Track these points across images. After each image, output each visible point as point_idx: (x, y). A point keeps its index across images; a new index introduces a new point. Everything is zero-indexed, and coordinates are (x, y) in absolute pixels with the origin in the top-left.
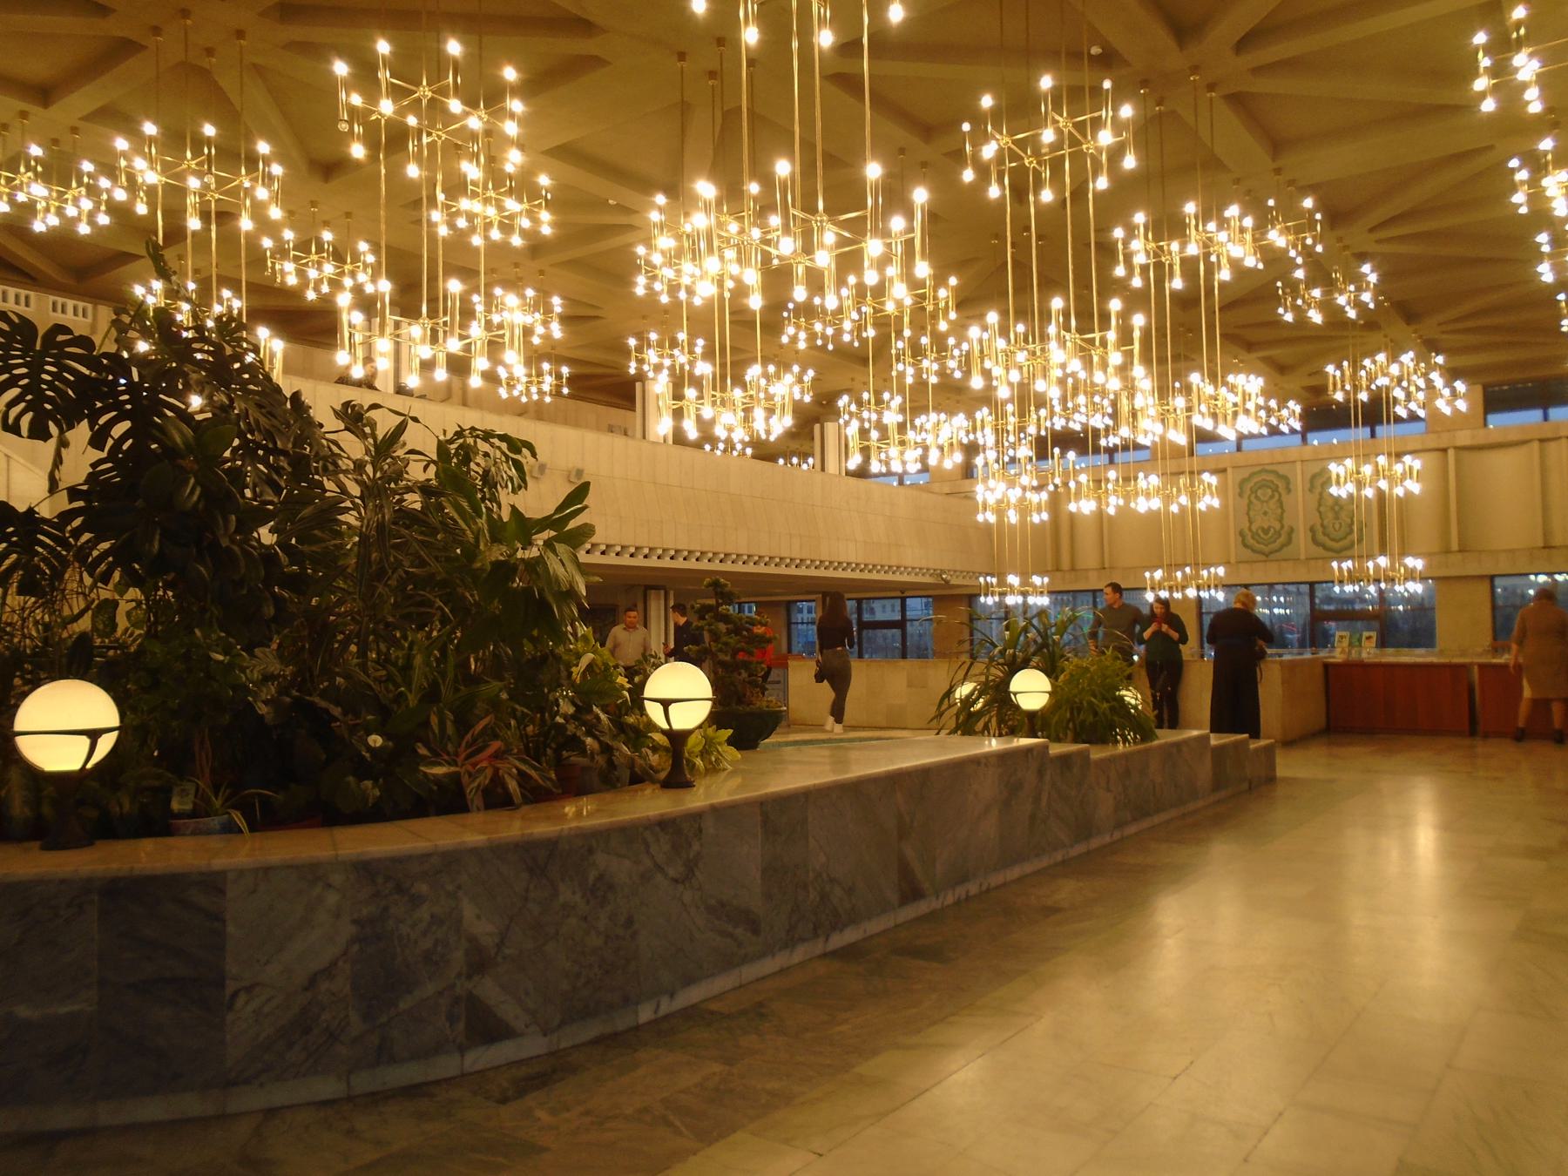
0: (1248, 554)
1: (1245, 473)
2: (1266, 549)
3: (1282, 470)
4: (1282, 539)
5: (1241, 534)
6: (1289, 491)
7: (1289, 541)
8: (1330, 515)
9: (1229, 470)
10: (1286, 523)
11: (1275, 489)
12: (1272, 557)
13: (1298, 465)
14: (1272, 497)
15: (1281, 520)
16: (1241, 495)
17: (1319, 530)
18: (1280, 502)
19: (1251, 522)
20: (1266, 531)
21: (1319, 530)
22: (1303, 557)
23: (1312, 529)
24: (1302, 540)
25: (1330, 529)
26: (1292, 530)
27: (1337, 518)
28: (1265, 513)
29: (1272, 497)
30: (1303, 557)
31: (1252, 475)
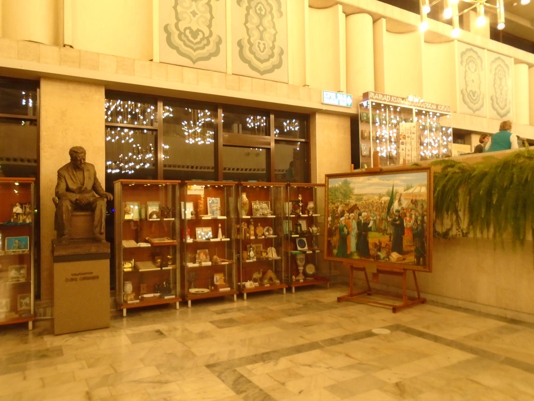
0: (174, 57)
2: (195, 54)
4: (211, 48)
5: (166, 28)
8: (256, 34)
12: (200, 64)
15: (210, 26)
17: (247, 46)
19: (178, 19)
20: (195, 34)
21: (247, 46)
22: (230, 71)
23: (240, 44)
24: (229, 49)
25: (255, 48)
27: (261, 38)
28: (194, 14)
30: (230, 71)
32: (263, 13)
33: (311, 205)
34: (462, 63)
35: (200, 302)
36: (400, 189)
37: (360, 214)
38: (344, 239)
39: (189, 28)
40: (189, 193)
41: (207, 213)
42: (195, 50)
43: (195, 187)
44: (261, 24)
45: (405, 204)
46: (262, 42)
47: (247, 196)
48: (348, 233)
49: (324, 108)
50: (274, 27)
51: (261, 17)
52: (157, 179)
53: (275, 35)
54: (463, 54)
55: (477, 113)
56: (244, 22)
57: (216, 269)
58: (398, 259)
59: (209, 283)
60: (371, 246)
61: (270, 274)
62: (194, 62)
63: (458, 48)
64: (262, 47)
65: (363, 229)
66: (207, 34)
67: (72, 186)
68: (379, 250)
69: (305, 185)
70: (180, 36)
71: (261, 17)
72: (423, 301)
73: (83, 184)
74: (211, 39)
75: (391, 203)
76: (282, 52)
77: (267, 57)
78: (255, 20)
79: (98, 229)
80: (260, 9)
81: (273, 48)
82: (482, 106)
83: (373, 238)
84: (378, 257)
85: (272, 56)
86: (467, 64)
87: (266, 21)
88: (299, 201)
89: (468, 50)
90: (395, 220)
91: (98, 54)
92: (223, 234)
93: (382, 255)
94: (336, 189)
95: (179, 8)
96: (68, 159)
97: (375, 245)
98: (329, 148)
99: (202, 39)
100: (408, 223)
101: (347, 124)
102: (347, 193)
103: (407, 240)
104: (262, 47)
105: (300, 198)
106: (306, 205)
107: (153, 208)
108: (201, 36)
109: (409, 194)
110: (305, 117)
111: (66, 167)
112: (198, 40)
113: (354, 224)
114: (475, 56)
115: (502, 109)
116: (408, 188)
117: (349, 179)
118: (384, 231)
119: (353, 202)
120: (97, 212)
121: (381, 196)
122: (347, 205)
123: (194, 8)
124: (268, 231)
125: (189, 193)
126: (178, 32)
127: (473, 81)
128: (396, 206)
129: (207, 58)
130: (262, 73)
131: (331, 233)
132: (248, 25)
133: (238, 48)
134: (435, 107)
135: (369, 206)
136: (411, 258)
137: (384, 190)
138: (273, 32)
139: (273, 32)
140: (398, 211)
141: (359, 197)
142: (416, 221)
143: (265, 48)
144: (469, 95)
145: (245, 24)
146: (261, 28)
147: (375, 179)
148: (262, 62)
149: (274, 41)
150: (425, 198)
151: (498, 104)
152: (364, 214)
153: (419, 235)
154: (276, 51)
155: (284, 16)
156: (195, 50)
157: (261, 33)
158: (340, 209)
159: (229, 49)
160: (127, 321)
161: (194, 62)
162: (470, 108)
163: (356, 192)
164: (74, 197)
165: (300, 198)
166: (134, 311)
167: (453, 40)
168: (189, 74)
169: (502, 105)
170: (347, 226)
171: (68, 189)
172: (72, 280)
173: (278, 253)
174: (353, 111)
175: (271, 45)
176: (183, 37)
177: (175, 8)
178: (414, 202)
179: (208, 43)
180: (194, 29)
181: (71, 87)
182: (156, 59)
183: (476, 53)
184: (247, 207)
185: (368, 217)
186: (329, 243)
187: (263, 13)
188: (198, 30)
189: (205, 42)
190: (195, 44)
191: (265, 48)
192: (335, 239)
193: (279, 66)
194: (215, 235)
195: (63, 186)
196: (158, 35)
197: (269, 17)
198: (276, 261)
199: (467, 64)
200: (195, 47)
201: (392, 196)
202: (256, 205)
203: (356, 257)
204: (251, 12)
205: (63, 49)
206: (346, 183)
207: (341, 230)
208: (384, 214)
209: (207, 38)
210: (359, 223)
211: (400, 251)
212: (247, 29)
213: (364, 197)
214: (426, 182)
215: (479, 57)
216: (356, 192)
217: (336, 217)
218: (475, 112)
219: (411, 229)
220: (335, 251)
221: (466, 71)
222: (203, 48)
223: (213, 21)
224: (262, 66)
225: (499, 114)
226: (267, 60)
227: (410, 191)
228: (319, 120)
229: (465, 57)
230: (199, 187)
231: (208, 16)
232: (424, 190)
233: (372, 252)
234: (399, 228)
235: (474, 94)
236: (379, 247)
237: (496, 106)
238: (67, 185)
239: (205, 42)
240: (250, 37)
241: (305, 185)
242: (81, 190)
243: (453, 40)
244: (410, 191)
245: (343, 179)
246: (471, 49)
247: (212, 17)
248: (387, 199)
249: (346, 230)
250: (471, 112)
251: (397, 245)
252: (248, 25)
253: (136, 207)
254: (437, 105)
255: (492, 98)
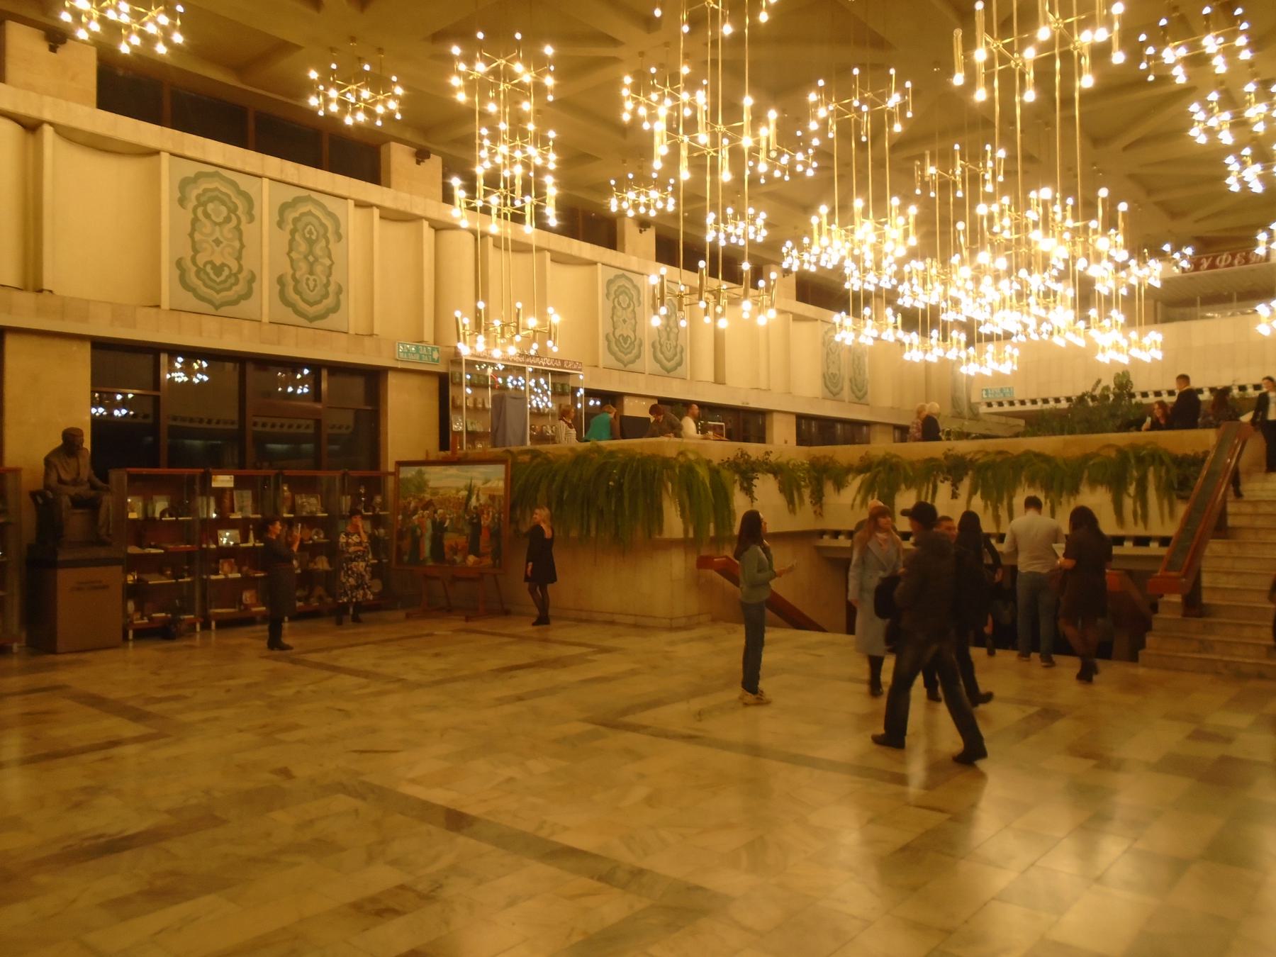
0: (191, 302)
1: (191, 169)
2: (218, 298)
3: (244, 183)
4: (240, 288)
5: (179, 264)
6: (251, 219)
7: (247, 295)
8: (303, 266)
9: (165, 157)
10: (248, 264)
11: (233, 210)
12: (225, 310)
13: (266, 181)
14: (227, 220)
15: (239, 259)
16: (182, 201)
17: (291, 283)
18: (238, 228)
19: (196, 251)
20: (218, 270)
22: (265, 319)
23: (281, 281)
24: (266, 288)
26: (252, 278)
27: (311, 273)
28: (218, 242)
29: (227, 220)
30: (265, 319)
31: (200, 175)
32: (314, 237)
33: (378, 499)
34: (608, 295)
35: (226, 624)
36: (478, 483)
37: (435, 512)
38: (416, 543)
39: (211, 262)
40: (214, 485)
41: (233, 511)
42: (218, 292)
43: (220, 478)
44: (311, 252)
45: (483, 499)
46: (312, 278)
47: (290, 489)
48: (422, 535)
49: (400, 365)
50: (330, 257)
51: (311, 243)
52: (157, 466)
53: (330, 267)
54: (610, 283)
55: (630, 367)
56: (287, 250)
57: (246, 582)
58: (475, 563)
59: (236, 601)
60: (446, 550)
61: (319, 591)
62: (217, 308)
63: (602, 274)
64: (312, 284)
65: (439, 528)
66: (235, 269)
67: (64, 476)
68: (456, 554)
69: (374, 473)
70: (197, 274)
71: (311, 243)
72: (507, 613)
73: (78, 474)
74: (240, 276)
75: (469, 498)
76: (340, 290)
77: (318, 298)
78: (303, 247)
79: (103, 531)
80: (310, 232)
81: (327, 284)
82: (638, 356)
83: (450, 539)
84: (454, 561)
85: (326, 295)
86: (617, 296)
87: (318, 250)
88: (360, 495)
89: (617, 277)
90: (472, 518)
91: (88, 301)
92: (256, 538)
93: (458, 559)
94: (408, 480)
95: (197, 236)
96: (59, 442)
97: (451, 548)
98: (406, 420)
99: (228, 277)
100: (486, 521)
101: (434, 385)
102: (421, 485)
103: (484, 540)
104: (312, 284)
105: (362, 491)
106: (370, 499)
107: (160, 505)
108: (226, 272)
109: (489, 489)
110: (374, 378)
111: (56, 452)
112: (222, 278)
113: (429, 524)
114: (628, 285)
115: (669, 360)
116: (487, 481)
117: (424, 468)
118: (460, 531)
119: (427, 497)
120: (103, 511)
121: (458, 490)
122: (421, 500)
123: (217, 234)
124: (317, 534)
125: (214, 485)
126: (194, 269)
127: (624, 321)
128: (473, 502)
129: (235, 302)
130: (311, 320)
131: (401, 535)
132: (293, 255)
133: (278, 287)
134: (559, 364)
135: (445, 502)
136: (488, 561)
137: (462, 483)
138: (328, 262)
139: (328, 262)
140: (475, 508)
141: (435, 491)
142: (493, 518)
143: (315, 286)
144: (617, 341)
145: (288, 254)
146: (311, 258)
147: (453, 470)
148: (311, 304)
149: (330, 274)
150: (502, 493)
151: (662, 353)
152: (440, 511)
153: (496, 534)
154: (332, 289)
155: (343, 240)
156: (218, 292)
157: (311, 265)
158: (413, 505)
159: (266, 288)
160: (134, 647)
161: (217, 308)
162: (618, 360)
163: (431, 484)
164: (73, 491)
165: (362, 491)
166: (143, 634)
167: (595, 263)
168: (210, 324)
169: (669, 354)
170: (421, 525)
171: (61, 481)
172: (79, 589)
173: (330, 563)
174: (441, 368)
175: (325, 281)
176: (205, 277)
177: (191, 235)
178: (492, 498)
179: (237, 283)
180: (218, 263)
181: (46, 341)
182: (165, 305)
183: (631, 280)
184: (289, 503)
185: (444, 514)
186: (399, 548)
187: (314, 237)
188: (223, 265)
189: (232, 280)
190: (219, 284)
191: (315, 286)
192: (406, 544)
193: (335, 309)
194: (245, 539)
195: (54, 477)
196: (167, 272)
197: (323, 243)
198: (327, 572)
199: (617, 296)
200: (218, 287)
201: (470, 490)
202: (300, 500)
203: (430, 563)
204: (297, 237)
205: (40, 296)
206: (420, 473)
207: (414, 531)
208: (461, 512)
209: (235, 275)
210: (434, 523)
211: (477, 554)
212: (292, 260)
213: (441, 492)
214: (503, 476)
215: (635, 286)
216: (431, 484)
217: (408, 514)
218: (625, 367)
219: (488, 527)
220: (406, 558)
221: (614, 308)
222: (229, 289)
223: (244, 252)
224: (311, 311)
225: (663, 367)
226: (320, 302)
227: (488, 485)
228: (393, 381)
229: (614, 288)
230: (227, 478)
231: (237, 244)
232: (501, 484)
233: (447, 557)
234: (476, 527)
235: (626, 339)
236: (455, 550)
237: (660, 356)
238: (59, 475)
239: (232, 280)
240: (294, 270)
241: (374, 473)
242: (75, 482)
243: (595, 263)
244: (488, 485)
245: (417, 468)
246: (623, 276)
247: (242, 246)
248: (464, 493)
249: (419, 531)
250: (621, 366)
251: (474, 548)
252: (293, 255)
253: (140, 504)
254: (562, 361)
255: (653, 345)
